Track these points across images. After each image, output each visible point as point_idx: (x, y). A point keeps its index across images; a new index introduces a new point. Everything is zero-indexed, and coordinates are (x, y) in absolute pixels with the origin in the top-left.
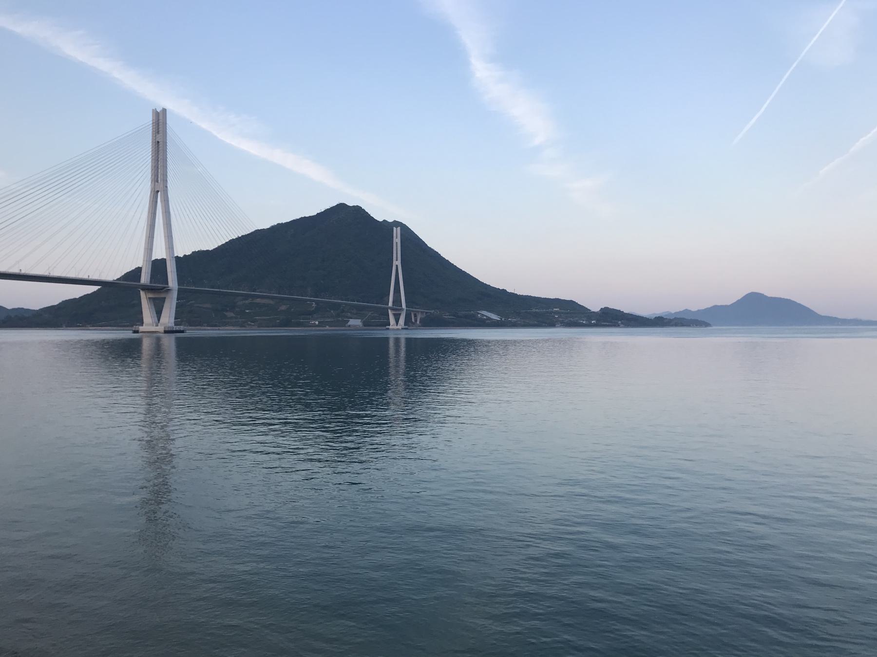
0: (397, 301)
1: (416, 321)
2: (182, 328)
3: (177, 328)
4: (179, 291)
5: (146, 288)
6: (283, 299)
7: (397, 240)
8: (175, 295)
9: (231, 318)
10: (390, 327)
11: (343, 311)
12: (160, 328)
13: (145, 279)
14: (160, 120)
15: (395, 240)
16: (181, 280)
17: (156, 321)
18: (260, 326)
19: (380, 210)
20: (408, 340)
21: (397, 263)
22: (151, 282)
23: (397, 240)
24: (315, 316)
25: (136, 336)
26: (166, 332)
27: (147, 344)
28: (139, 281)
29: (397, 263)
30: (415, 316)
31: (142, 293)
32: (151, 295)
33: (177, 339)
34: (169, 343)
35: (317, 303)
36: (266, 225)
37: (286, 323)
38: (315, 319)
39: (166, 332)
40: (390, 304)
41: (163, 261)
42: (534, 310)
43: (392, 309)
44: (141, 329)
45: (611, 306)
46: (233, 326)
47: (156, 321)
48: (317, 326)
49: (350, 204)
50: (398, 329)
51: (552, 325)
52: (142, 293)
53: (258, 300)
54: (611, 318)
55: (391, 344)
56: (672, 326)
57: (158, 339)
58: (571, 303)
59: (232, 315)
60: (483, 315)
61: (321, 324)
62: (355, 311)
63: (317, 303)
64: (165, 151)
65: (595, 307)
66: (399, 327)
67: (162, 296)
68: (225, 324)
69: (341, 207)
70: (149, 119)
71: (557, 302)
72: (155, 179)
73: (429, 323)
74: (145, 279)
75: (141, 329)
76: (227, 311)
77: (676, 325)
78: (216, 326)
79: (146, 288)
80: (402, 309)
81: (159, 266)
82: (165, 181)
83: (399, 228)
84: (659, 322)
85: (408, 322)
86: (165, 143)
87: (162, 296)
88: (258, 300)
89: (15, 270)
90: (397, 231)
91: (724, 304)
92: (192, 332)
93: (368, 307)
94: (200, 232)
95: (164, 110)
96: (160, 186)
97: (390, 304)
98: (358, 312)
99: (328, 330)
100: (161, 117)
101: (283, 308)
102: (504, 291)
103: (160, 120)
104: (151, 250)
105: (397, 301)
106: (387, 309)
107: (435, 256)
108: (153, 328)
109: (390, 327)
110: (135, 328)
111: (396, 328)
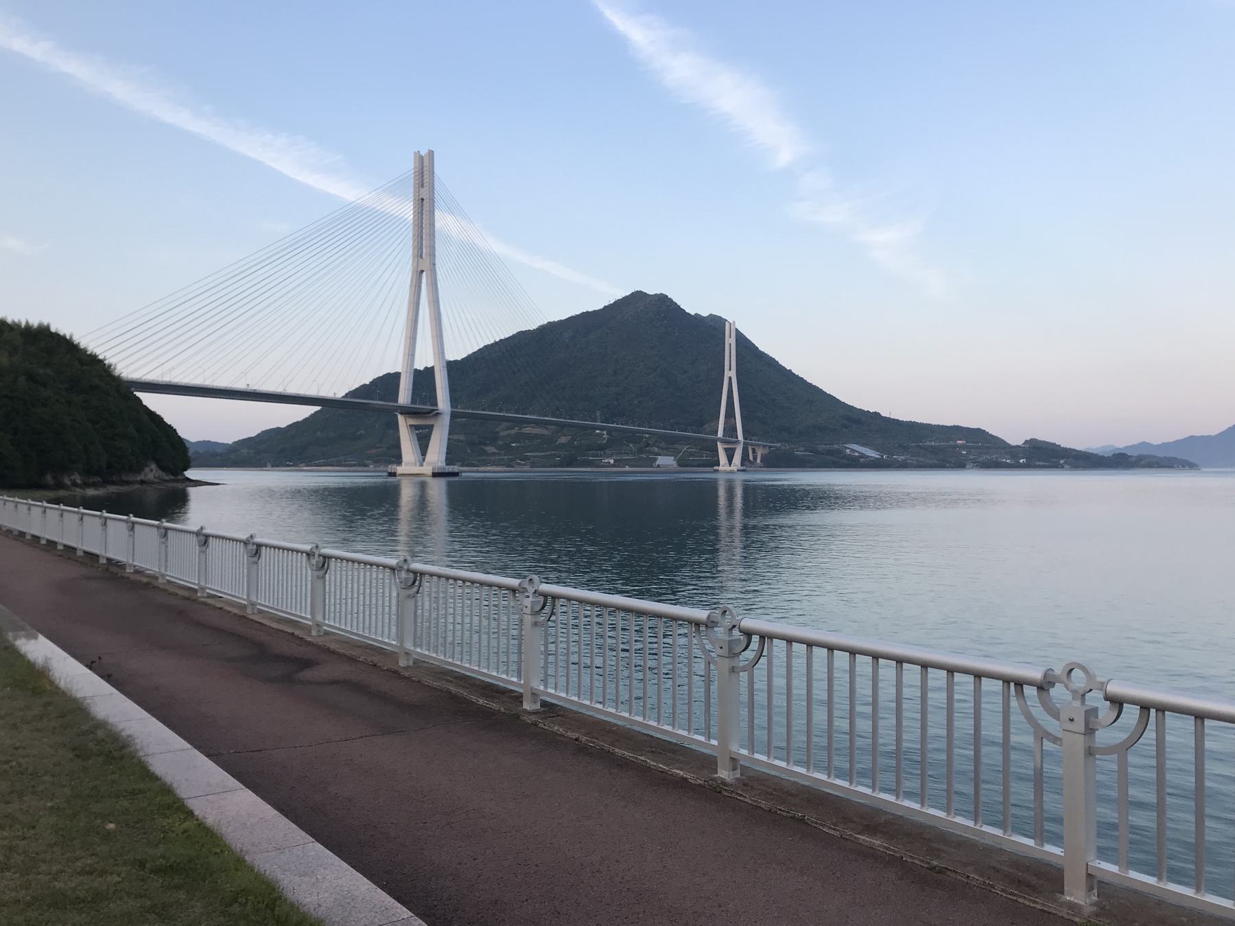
0: (730, 430)
1: (755, 458)
2: (456, 468)
3: (450, 469)
4: (454, 416)
5: (407, 412)
6: (563, 426)
7: (730, 341)
8: (446, 420)
9: (494, 454)
10: (720, 468)
11: (648, 445)
12: (427, 469)
13: (404, 397)
14: (424, 172)
16: (454, 400)
17: (420, 461)
18: (533, 465)
20: (748, 489)
21: (730, 373)
22: (413, 401)
24: (608, 451)
25: (391, 479)
26: (435, 475)
27: (407, 493)
29: (730, 373)
30: (754, 451)
31: (401, 419)
32: (412, 422)
33: (449, 485)
34: (438, 491)
35: (609, 431)
36: (532, 325)
37: (570, 462)
38: (610, 456)
39: (435, 475)
40: (720, 434)
41: (429, 371)
42: (928, 443)
43: (723, 442)
44: (400, 470)
45: (1042, 436)
46: (498, 465)
47: (420, 461)
48: (613, 466)
49: (651, 291)
50: (732, 472)
51: (960, 465)
52: (401, 419)
53: (528, 430)
54: (1042, 456)
55: (722, 493)
56: (1143, 467)
57: (423, 486)
58: (979, 433)
59: (493, 450)
60: (853, 450)
61: (618, 463)
62: (663, 445)
63: (609, 431)
64: (432, 212)
65: (1015, 439)
66: (733, 468)
67: (428, 422)
68: (485, 463)
69: (638, 296)
70: (409, 166)
71: (957, 429)
72: (419, 255)
73: (775, 461)
74: (404, 397)
75: (400, 470)
76: (486, 445)
77: (1170, 467)
78: (474, 465)
79: (407, 412)
80: (738, 442)
81: (424, 379)
82: (432, 255)
84: (1119, 461)
85: (745, 459)
86: (432, 200)
87: (428, 422)
88: (528, 430)
89: (240, 385)
91: (1206, 434)
92: (470, 474)
93: (685, 438)
94: (471, 329)
95: (431, 153)
96: (425, 264)
97: (720, 434)
98: (669, 445)
99: (632, 474)
100: (426, 163)
101: (563, 440)
103: (424, 172)
104: (443, 353)
105: (730, 430)
106: (715, 441)
107: (771, 363)
108: (416, 470)
109: (720, 468)
110: (391, 468)
111: (728, 468)
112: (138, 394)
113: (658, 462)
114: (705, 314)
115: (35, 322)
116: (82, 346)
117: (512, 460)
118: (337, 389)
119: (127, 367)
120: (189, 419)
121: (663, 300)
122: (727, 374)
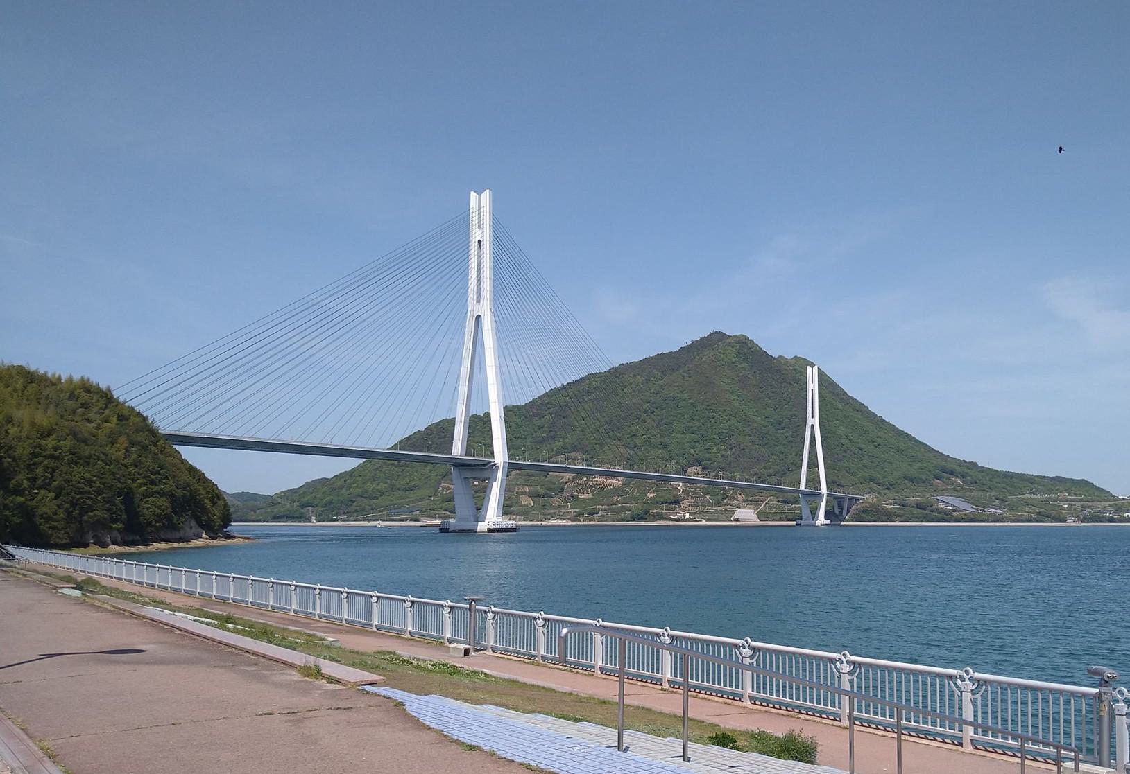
0: (813, 480)
5: (460, 465)
7: (813, 386)
13: (458, 450)
15: (810, 386)
19: (777, 343)
21: (813, 420)
23: (813, 386)
28: (450, 451)
29: (813, 420)
36: (604, 369)
40: (802, 486)
48: (687, 520)
58: (1083, 484)
71: (1059, 482)
80: (821, 495)
83: (815, 369)
90: (812, 375)
97: (802, 486)
102: (974, 465)
107: (861, 409)
109: (802, 522)
112: (177, 447)
113: (736, 515)
114: (789, 356)
115: (77, 377)
116: (122, 399)
117: (579, 514)
118: (383, 443)
119: (166, 424)
120: (228, 473)
121: (743, 342)
122: (810, 421)
